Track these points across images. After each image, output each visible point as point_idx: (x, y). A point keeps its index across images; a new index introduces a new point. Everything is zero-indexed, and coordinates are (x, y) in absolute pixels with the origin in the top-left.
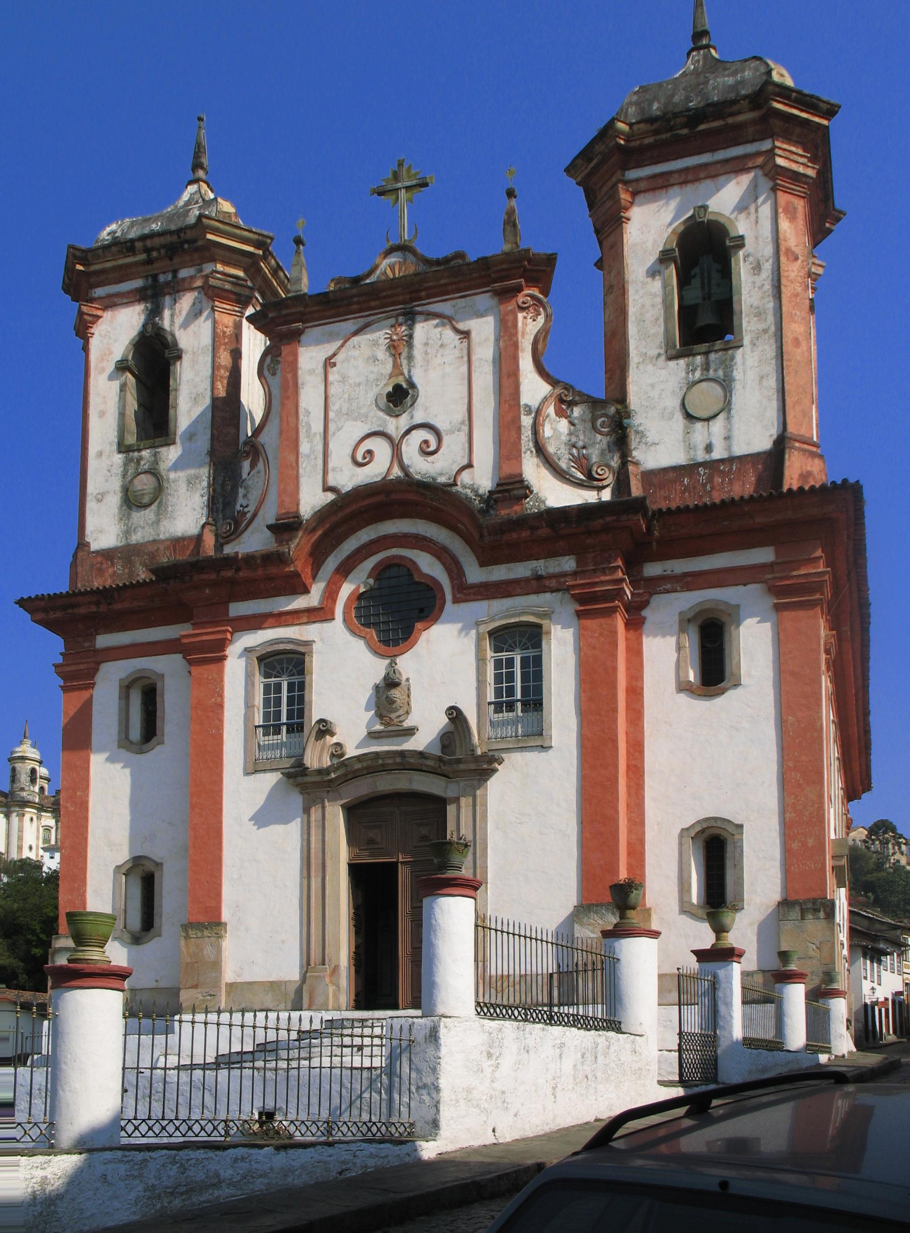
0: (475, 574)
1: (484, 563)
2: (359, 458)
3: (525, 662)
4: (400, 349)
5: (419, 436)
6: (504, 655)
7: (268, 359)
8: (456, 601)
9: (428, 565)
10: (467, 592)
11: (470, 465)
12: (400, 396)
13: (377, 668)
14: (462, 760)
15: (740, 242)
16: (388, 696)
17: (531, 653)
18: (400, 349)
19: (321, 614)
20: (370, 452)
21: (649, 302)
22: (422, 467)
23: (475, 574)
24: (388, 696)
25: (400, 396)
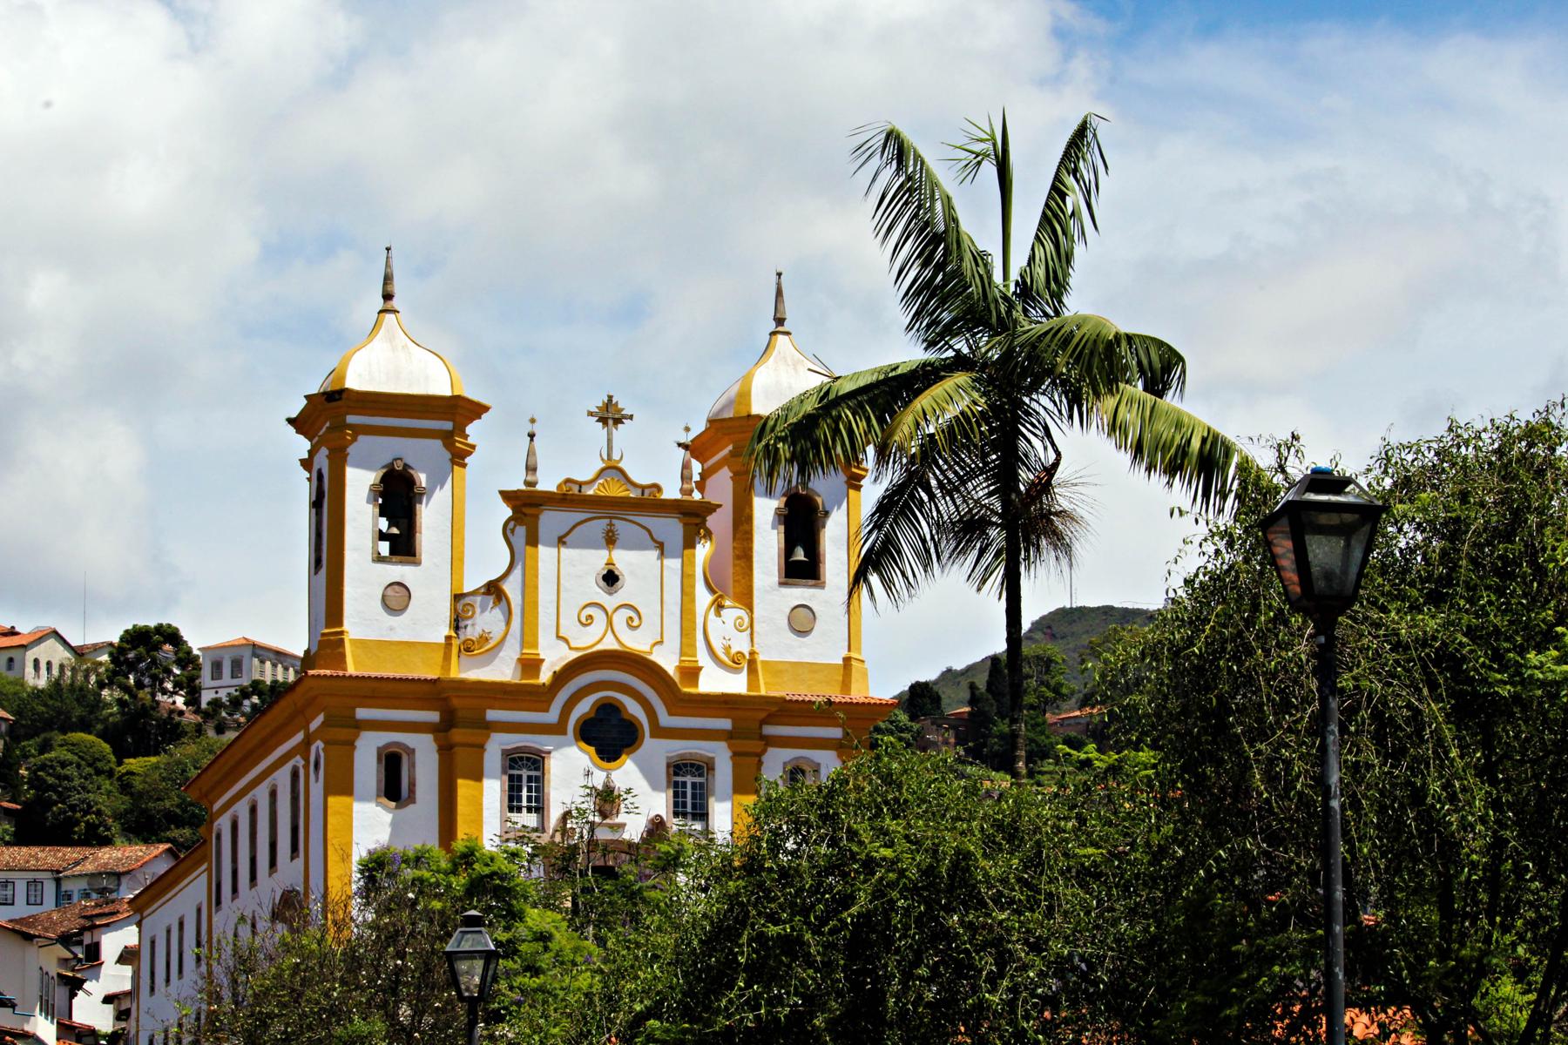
0: (665, 719)
1: (670, 714)
2: (583, 620)
3: (694, 785)
5: (626, 613)
6: (680, 779)
7: (512, 524)
8: (652, 736)
9: (633, 708)
10: (660, 732)
11: (661, 642)
12: (611, 579)
17: (698, 780)
19: (558, 729)
20: (590, 617)
21: (768, 541)
25: (611, 579)
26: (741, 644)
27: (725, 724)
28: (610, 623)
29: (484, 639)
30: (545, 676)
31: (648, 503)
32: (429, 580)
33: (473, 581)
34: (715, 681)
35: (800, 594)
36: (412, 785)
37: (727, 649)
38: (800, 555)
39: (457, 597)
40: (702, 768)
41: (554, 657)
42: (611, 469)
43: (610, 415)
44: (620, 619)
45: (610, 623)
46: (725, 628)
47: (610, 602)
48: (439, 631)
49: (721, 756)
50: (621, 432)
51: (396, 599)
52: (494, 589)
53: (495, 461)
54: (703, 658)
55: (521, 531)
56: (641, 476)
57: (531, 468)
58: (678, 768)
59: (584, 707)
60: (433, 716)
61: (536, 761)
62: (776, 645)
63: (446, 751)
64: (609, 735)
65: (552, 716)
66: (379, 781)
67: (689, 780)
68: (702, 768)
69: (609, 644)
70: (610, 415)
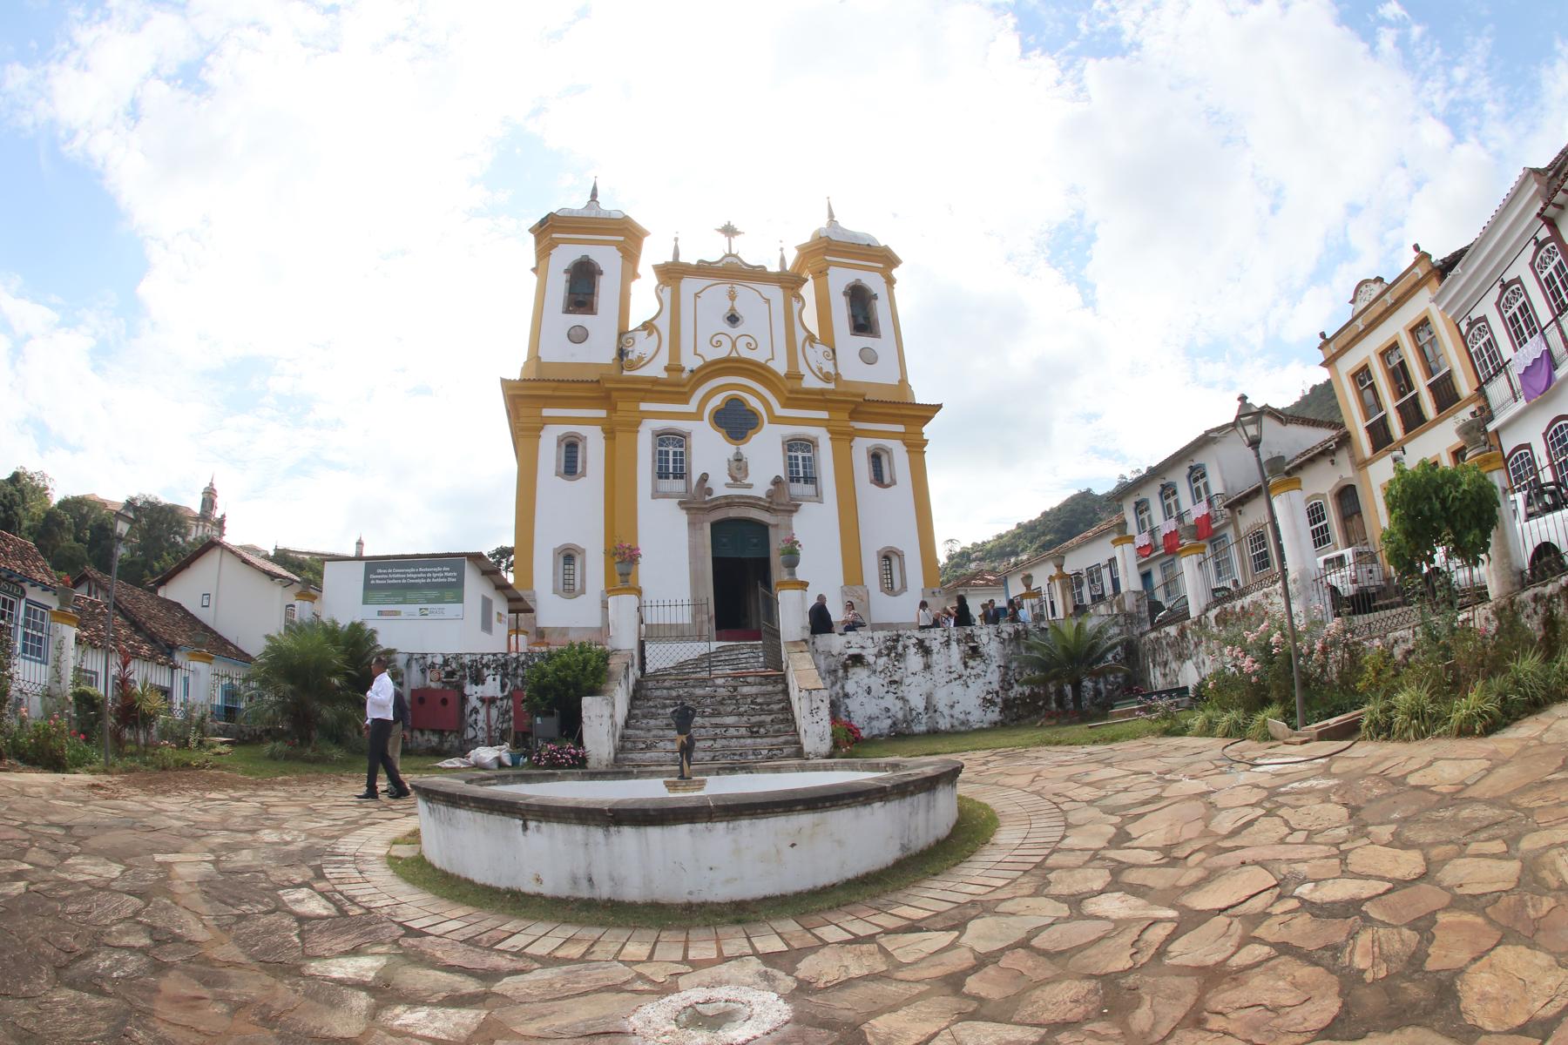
0: (779, 411)
1: (784, 406)
4: (732, 297)
9: (754, 403)
12: (733, 319)
13: (728, 449)
14: (781, 501)
15: (875, 297)
16: (738, 467)
18: (732, 297)
19: (697, 416)
22: (746, 354)
23: (779, 411)
24: (738, 467)
25: (733, 319)
26: (828, 367)
27: (824, 415)
28: (734, 345)
29: (640, 358)
30: (685, 375)
31: (757, 275)
32: (601, 325)
33: (634, 322)
34: (811, 382)
35: (864, 341)
36: (584, 462)
37: (820, 369)
38: (861, 320)
39: (623, 333)
40: (808, 444)
41: (690, 362)
42: (730, 255)
43: (729, 231)
44: (741, 344)
45: (734, 345)
46: (816, 356)
47: (734, 332)
48: (607, 356)
49: (822, 436)
50: (736, 240)
51: (578, 336)
52: (648, 326)
53: (653, 253)
54: (803, 369)
55: (668, 290)
56: (751, 258)
57: (676, 254)
58: (792, 445)
59: (717, 401)
60: (602, 413)
61: (681, 438)
62: (854, 371)
63: (610, 435)
64: (736, 422)
65: (692, 407)
66: (558, 460)
67: (800, 455)
68: (808, 444)
69: (734, 355)
70: (729, 231)
